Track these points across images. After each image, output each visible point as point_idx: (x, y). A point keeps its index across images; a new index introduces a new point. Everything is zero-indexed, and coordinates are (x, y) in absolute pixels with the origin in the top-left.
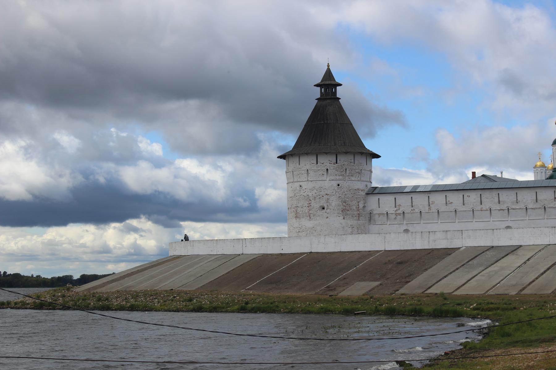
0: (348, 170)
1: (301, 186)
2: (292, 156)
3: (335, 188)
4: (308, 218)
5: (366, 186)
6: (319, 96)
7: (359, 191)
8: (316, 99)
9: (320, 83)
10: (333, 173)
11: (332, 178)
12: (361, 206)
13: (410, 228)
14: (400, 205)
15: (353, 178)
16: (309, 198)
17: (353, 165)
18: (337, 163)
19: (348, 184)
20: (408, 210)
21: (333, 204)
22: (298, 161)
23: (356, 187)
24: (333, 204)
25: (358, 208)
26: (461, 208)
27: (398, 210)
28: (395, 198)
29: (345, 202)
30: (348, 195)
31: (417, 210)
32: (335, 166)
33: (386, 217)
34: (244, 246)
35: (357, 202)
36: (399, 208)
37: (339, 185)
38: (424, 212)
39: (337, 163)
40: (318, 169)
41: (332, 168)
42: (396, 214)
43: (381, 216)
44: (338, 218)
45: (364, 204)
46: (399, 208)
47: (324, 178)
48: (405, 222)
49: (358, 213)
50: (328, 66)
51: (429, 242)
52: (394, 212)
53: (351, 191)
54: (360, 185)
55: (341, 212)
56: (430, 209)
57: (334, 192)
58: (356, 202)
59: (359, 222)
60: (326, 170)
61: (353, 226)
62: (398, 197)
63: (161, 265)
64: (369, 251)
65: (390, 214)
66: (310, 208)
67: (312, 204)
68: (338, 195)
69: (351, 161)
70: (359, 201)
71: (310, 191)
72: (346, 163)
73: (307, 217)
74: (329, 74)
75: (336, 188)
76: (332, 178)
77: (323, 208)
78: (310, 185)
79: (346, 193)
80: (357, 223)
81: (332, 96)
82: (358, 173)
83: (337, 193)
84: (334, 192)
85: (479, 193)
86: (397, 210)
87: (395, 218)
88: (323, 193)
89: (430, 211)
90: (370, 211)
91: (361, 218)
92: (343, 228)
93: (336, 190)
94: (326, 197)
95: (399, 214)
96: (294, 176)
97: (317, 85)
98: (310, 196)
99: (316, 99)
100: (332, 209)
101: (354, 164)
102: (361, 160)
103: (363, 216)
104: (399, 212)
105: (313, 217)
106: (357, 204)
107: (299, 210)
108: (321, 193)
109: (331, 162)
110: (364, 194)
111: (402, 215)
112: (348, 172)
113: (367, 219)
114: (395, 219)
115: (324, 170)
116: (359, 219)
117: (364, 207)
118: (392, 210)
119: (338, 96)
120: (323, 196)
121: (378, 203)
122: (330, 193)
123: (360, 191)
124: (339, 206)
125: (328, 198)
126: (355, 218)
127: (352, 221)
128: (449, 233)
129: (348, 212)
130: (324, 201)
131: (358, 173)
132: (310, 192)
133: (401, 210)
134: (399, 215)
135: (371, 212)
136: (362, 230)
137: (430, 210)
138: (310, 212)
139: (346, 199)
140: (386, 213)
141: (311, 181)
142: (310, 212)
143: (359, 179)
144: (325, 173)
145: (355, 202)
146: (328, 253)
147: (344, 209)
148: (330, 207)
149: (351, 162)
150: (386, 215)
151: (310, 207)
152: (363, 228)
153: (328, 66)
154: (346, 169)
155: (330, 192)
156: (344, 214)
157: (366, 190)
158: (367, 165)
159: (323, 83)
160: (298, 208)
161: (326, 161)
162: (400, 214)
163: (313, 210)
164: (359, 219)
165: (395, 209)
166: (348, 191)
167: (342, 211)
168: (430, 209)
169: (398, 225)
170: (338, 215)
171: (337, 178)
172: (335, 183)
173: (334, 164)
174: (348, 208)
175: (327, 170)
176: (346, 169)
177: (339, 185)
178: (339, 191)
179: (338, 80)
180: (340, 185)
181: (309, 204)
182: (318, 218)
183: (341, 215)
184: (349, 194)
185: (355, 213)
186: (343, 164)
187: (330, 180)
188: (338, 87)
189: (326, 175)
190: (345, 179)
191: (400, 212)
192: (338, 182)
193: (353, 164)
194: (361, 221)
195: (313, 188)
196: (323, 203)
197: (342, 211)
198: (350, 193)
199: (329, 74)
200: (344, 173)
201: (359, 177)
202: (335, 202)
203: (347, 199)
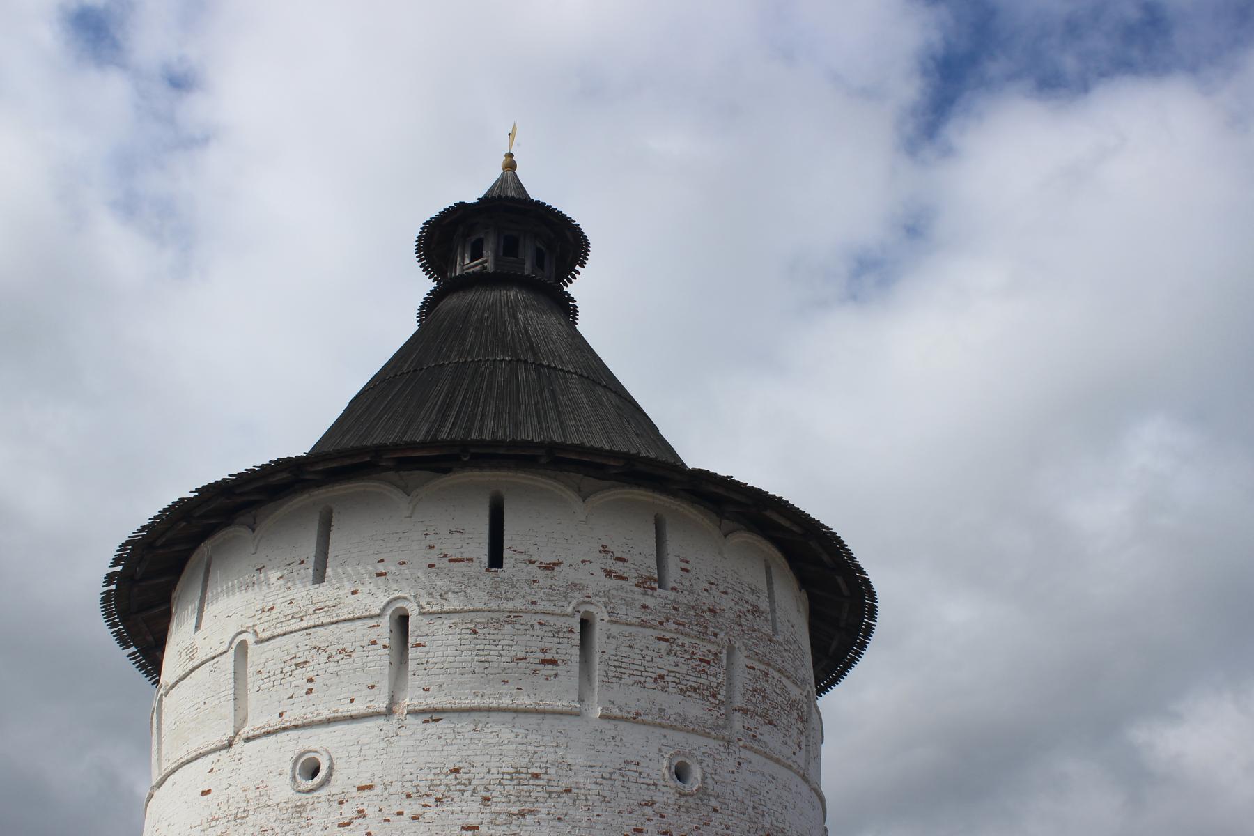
2: (253, 530)
3: (660, 799)
22: (309, 549)
32: (650, 602)
40: (509, 605)
71: (412, 808)
93: (669, 812)
96: (253, 681)
109: (618, 567)
115: (559, 622)
132: (416, 818)
153: (510, 165)
180: (696, 773)
186: (708, 600)
187: (616, 712)
189: (575, 666)
195: (450, 779)
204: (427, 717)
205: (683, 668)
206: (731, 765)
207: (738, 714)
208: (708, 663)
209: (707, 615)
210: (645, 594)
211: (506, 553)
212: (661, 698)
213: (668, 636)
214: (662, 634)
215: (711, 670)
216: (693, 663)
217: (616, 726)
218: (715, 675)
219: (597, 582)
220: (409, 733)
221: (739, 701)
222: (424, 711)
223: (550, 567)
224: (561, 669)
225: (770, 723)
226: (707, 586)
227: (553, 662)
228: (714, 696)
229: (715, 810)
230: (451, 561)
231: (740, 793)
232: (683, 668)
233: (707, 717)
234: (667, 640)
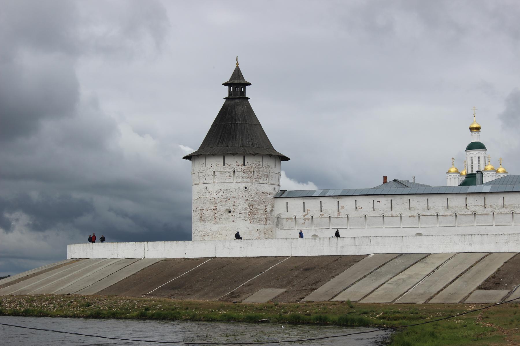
0: (255, 172)
1: (207, 188)
2: (198, 157)
3: (242, 191)
4: (214, 221)
5: (274, 189)
6: (227, 96)
7: (267, 195)
8: (224, 99)
9: (229, 81)
10: (240, 175)
11: (240, 180)
12: (269, 210)
13: (319, 234)
14: (308, 210)
15: (261, 181)
16: (215, 201)
18: (244, 165)
19: (255, 187)
20: (316, 214)
21: (240, 208)
22: (204, 162)
23: (264, 190)
24: (240, 208)
25: (266, 212)
26: (370, 214)
27: (307, 214)
29: (252, 206)
30: (256, 198)
31: (326, 215)
32: (242, 168)
33: (294, 222)
34: (146, 249)
36: (308, 213)
37: (246, 188)
38: (333, 217)
39: (244, 165)
40: (225, 170)
41: (239, 170)
42: (305, 219)
43: (289, 221)
44: (245, 221)
45: (272, 207)
46: (308, 213)
47: (231, 180)
48: (313, 228)
49: (266, 217)
50: (237, 65)
51: (337, 248)
52: (302, 217)
53: (259, 194)
54: (268, 189)
55: (247, 216)
56: (339, 214)
59: (266, 226)
60: (233, 172)
62: (307, 201)
63: (58, 268)
64: (276, 257)
66: (216, 211)
67: (217, 207)
68: (245, 198)
69: (259, 163)
71: (216, 194)
72: (254, 165)
73: (213, 220)
74: (237, 73)
75: (243, 191)
76: (240, 180)
77: (230, 212)
78: (217, 187)
79: (253, 196)
80: (265, 227)
81: (240, 95)
82: (266, 176)
83: (244, 196)
84: (241, 195)
85: (389, 198)
86: (305, 215)
87: (304, 223)
88: (229, 196)
89: (339, 216)
90: (278, 215)
91: (268, 222)
94: (233, 200)
95: (308, 219)
96: (200, 177)
97: (225, 84)
98: (216, 198)
99: (224, 99)
100: (239, 213)
101: (262, 166)
102: (268, 163)
103: (271, 220)
105: (219, 221)
106: (264, 207)
107: (204, 212)
108: (227, 196)
109: (238, 164)
110: (272, 197)
111: (310, 219)
112: (255, 174)
113: (275, 223)
114: (303, 223)
116: (266, 223)
117: (272, 211)
118: (300, 215)
119: (247, 96)
120: (229, 199)
121: (286, 207)
122: (236, 196)
123: (268, 195)
126: (262, 222)
128: (357, 239)
129: (255, 216)
130: (231, 204)
131: (266, 176)
133: (309, 214)
135: (279, 216)
136: (269, 235)
137: (340, 215)
138: (216, 215)
140: (294, 217)
141: (218, 183)
142: (216, 215)
144: (232, 175)
145: (262, 206)
146: (233, 258)
147: (250, 213)
148: (237, 210)
149: (259, 165)
150: (294, 219)
151: (216, 210)
152: (270, 232)
153: (237, 65)
155: (236, 195)
156: (251, 218)
158: (275, 167)
159: (231, 82)
160: (203, 210)
161: (233, 162)
162: (308, 219)
163: (218, 213)
164: (266, 223)
165: (304, 214)
166: (256, 194)
167: (249, 215)
168: (339, 214)
171: (245, 181)
172: (242, 186)
173: (241, 166)
174: (255, 212)
175: (234, 171)
176: (254, 172)
177: (246, 188)
178: (246, 193)
179: (247, 79)
180: (247, 188)
181: (215, 207)
182: (224, 222)
183: (248, 219)
185: (262, 217)
188: (247, 87)
189: (233, 177)
190: (252, 182)
192: (246, 185)
193: (261, 166)
194: (269, 226)
195: (220, 190)
196: (229, 206)
197: (249, 215)
199: (237, 73)
200: (252, 175)
202: (241, 205)
203: (255, 203)
206: (253, 186)
211: (225, 164)
212: (243, 179)
221: (255, 177)
223: (230, 165)
224: (231, 177)
227: (230, 177)
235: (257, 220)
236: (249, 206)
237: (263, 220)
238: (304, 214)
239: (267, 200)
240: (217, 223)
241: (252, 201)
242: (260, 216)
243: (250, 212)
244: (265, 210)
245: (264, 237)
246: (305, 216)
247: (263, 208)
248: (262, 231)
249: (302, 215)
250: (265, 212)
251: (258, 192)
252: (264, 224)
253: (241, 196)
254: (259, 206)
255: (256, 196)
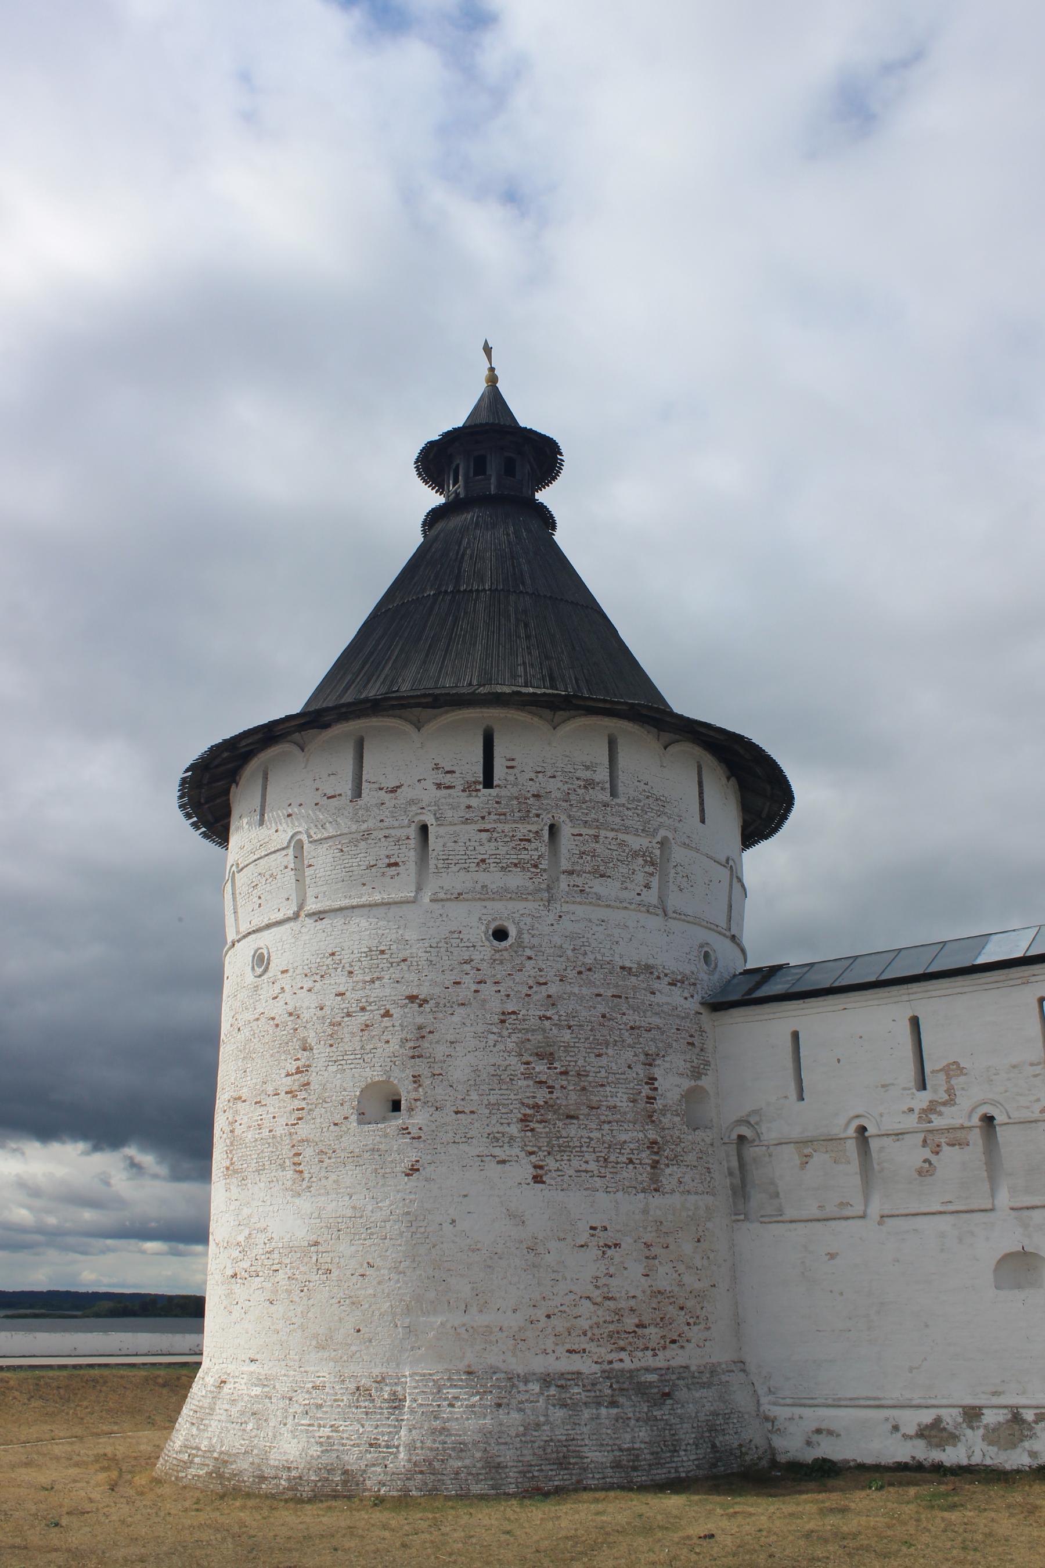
0: (566, 830)
3: (477, 957)
4: (290, 1174)
5: (706, 955)
7: (656, 985)
11: (456, 881)
14: (953, 1070)
16: (302, 1033)
17: (606, 805)
18: (488, 781)
23: (629, 954)
24: (460, 1069)
25: (650, 1099)
27: (944, 1104)
28: (915, 1022)
29: (547, 1056)
32: (474, 802)
33: (855, 1166)
35: (642, 1057)
36: (950, 1091)
40: (364, 826)
42: (933, 1142)
43: (819, 1159)
44: (493, 1169)
45: (697, 1073)
46: (950, 1091)
48: (1004, 1198)
49: (652, 1135)
52: (911, 1122)
53: (597, 976)
55: (514, 1130)
57: (468, 981)
58: (628, 1055)
59: (656, 1201)
60: (413, 832)
61: (610, 1237)
65: (887, 1141)
66: (303, 1104)
67: (313, 1077)
68: (495, 1005)
69: (588, 774)
70: (652, 1050)
71: (308, 984)
73: (283, 1167)
77: (396, 1106)
79: (553, 989)
80: (645, 1211)
82: (640, 861)
83: (488, 990)
84: (466, 979)
86: (932, 1108)
87: (927, 1170)
91: (670, 1175)
92: (530, 1249)
93: (484, 966)
95: (957, 1138)
98: (306, 1015)
100: (450, 1109)
101: (614, 794)
104: (948, 1118)
105: (315, 1169)
106: (639, 1069)
109: (448, 779)
110: (693, 1005)
111: (976, 1137)
114: (920, 1172)
116: (654, 1179)
117: (693, 1096)
120: (387, 1014)
121: (789, 1064)
122: (437, 991)
123: (662, 985)
124: (501, 1081)
125: (420, 1028)
126: (628, 1173)
127: (601, 1195)
129: (572, 1130)
131: (640, 861)
132: (310, 990)
133: (964, 1102)
134: (951, 1145)
135: (745, 1131)
136: (681, 1268)
139: (555, 1031)
140: (851, 1131)
143: (651, 897)
144: (409, 854)
147: (536, 1106)
150: (851, 1146)
151: (303, 1094)
152: (688, 1248)
153: (492, 379)
154: (553, 829)
156: (543, 1142)
157: (708, 981)
158: (703, 821)
160: (240, 1104)
162: (959, 1134)
164: (654, 1179)
165: (922, 1100)
166: (571, 974)
167: (525, 1119)
169: (948, 1217)
170: (497, 1151)
173: (469, 788)
174: (570, 1099)
176: (553, 829)
178: (500, 972)
180: (513, 932)
181: (298, 1071)
183: (516, 1151)
184: (582, 998)
185: (623, 1137)
186: (534, 788)
187: (442, 896)
189: (412, 867)
191: (957, 1122)
193: (605, 797)
194: (676, 1199)
195: (329, 961)
197: (525, 1119)
198: (585, 991)
200: (544, 849)
201: (647, 886)
203: (567, 1036)
204: (316, 917)
205: (503, 850)
206: (551, 918)
207: (563, 877)
208: (529, 841)
209: (532, 801)
210: (470, 796)
211: (364, 785)
212: (483, 877)
213: (488, 827)
214: (482, 827)
215: (533, 846)
216: (513, 844)
217: (443, 906)
218: (537, 849)
219: (429, 794)
220: (307, 930)
221: (565, 865)
222: (314, 914)
223: (393, 790)
224: (401, 869)
225: (602, 876)
226: (533, 775)
227: (396, 864)
228: (536, 866)
229: (530, 958)
230: (329, 798)
231: (557, 940)
232: (503, 850)
233: (529, 884)
234: (488, 831)
235: (587, 1156)
236: (526, 1058)
237: (631, 1161)
238: (925, 1105)
239: (656, 1021)
240: (305, 1184)
241: (547, 1023)
242: (606, 1127)
243: (531, 1102)
244: (646, 1090)
245: (645, 1282)
246: (933, 1117)
247: (631, 1075)
248: (627, 1243)
249: (911, 1110)
250: (641, 1105)
251: (589, 960)
252: (644, 1191)
253: (464, 993)
254: (599, 1055)
255: (576, 990)
